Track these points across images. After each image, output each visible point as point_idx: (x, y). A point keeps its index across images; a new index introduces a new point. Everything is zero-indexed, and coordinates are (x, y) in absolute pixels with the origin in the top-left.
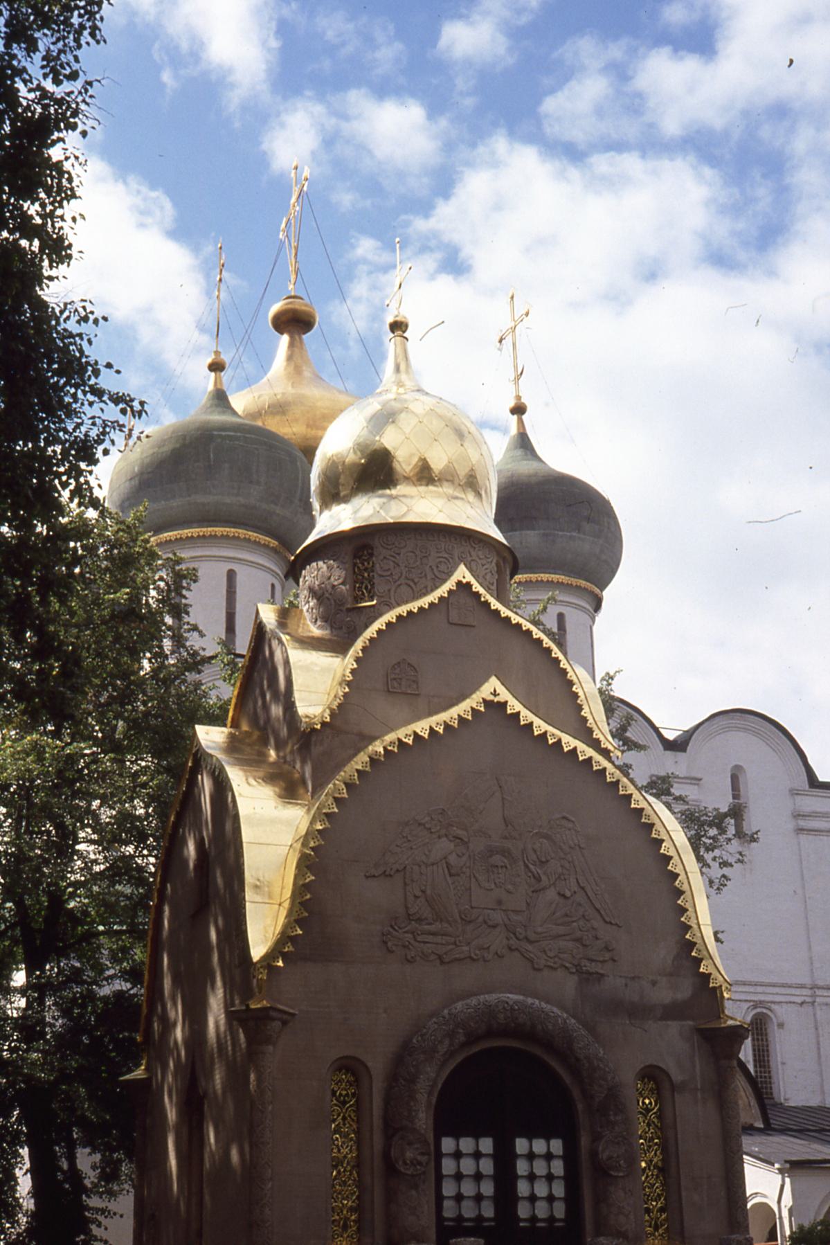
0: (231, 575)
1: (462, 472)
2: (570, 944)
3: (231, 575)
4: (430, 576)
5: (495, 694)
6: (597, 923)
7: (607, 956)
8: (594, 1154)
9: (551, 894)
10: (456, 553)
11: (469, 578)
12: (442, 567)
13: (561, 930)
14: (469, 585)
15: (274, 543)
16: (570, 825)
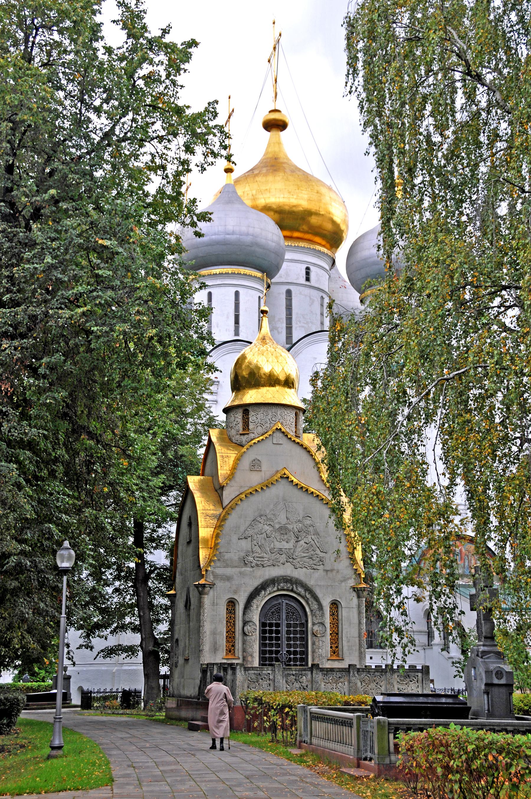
0: (237, 294)
1: (282, 378)
2: (308, 560)
3: (237, 294)
4: (269, 422)
5: (285, 474)
6: (318, 552)
7: (321, 563)
8: (312, 629)
9: (302, 542)
10: (279, 413)
11: (280, 426)
12: (274, 419)
13: (305, 555)
14: (280, 429)
15: (259, 274)
16: (310, 519)
